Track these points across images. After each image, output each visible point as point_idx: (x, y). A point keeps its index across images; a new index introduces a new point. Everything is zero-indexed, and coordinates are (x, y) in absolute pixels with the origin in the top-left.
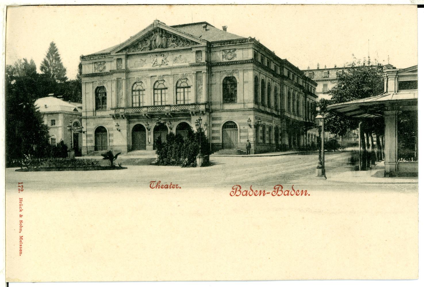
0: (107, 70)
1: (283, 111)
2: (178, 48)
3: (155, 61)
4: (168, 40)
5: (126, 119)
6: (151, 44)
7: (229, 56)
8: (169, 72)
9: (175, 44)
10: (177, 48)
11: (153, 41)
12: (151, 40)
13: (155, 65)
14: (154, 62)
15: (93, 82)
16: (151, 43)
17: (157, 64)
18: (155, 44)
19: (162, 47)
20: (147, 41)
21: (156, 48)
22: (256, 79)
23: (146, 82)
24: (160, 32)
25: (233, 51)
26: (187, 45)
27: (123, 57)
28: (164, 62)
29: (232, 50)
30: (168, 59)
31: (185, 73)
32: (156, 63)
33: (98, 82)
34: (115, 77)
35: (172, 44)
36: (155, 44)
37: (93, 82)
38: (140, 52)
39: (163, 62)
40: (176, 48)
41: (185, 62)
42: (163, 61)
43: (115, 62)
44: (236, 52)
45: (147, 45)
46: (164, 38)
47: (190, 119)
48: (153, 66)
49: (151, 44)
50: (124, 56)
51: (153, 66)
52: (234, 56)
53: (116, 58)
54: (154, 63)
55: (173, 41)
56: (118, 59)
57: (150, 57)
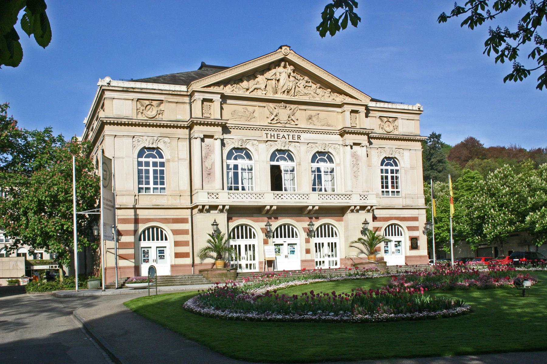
2: (317, 100)
4: (298, 84)
9: (313, 94)
12: (270, 78)
13: (274, 122)
15: (134, 137)
17: (278, 121)
24: (285, 67)
26: (331, 98)
27: (217, 98)
28: (292, 120)
30: (299, 114)
31: (327, 143)
32: (276, 118)
33: (147, 137)
38: (247, 94)
39: (290, 119)
40: (313, 99)
46: (292, 79)
48: (271, 123)
50: (219, 96)
51: (271, 123)
54: (274, 119)
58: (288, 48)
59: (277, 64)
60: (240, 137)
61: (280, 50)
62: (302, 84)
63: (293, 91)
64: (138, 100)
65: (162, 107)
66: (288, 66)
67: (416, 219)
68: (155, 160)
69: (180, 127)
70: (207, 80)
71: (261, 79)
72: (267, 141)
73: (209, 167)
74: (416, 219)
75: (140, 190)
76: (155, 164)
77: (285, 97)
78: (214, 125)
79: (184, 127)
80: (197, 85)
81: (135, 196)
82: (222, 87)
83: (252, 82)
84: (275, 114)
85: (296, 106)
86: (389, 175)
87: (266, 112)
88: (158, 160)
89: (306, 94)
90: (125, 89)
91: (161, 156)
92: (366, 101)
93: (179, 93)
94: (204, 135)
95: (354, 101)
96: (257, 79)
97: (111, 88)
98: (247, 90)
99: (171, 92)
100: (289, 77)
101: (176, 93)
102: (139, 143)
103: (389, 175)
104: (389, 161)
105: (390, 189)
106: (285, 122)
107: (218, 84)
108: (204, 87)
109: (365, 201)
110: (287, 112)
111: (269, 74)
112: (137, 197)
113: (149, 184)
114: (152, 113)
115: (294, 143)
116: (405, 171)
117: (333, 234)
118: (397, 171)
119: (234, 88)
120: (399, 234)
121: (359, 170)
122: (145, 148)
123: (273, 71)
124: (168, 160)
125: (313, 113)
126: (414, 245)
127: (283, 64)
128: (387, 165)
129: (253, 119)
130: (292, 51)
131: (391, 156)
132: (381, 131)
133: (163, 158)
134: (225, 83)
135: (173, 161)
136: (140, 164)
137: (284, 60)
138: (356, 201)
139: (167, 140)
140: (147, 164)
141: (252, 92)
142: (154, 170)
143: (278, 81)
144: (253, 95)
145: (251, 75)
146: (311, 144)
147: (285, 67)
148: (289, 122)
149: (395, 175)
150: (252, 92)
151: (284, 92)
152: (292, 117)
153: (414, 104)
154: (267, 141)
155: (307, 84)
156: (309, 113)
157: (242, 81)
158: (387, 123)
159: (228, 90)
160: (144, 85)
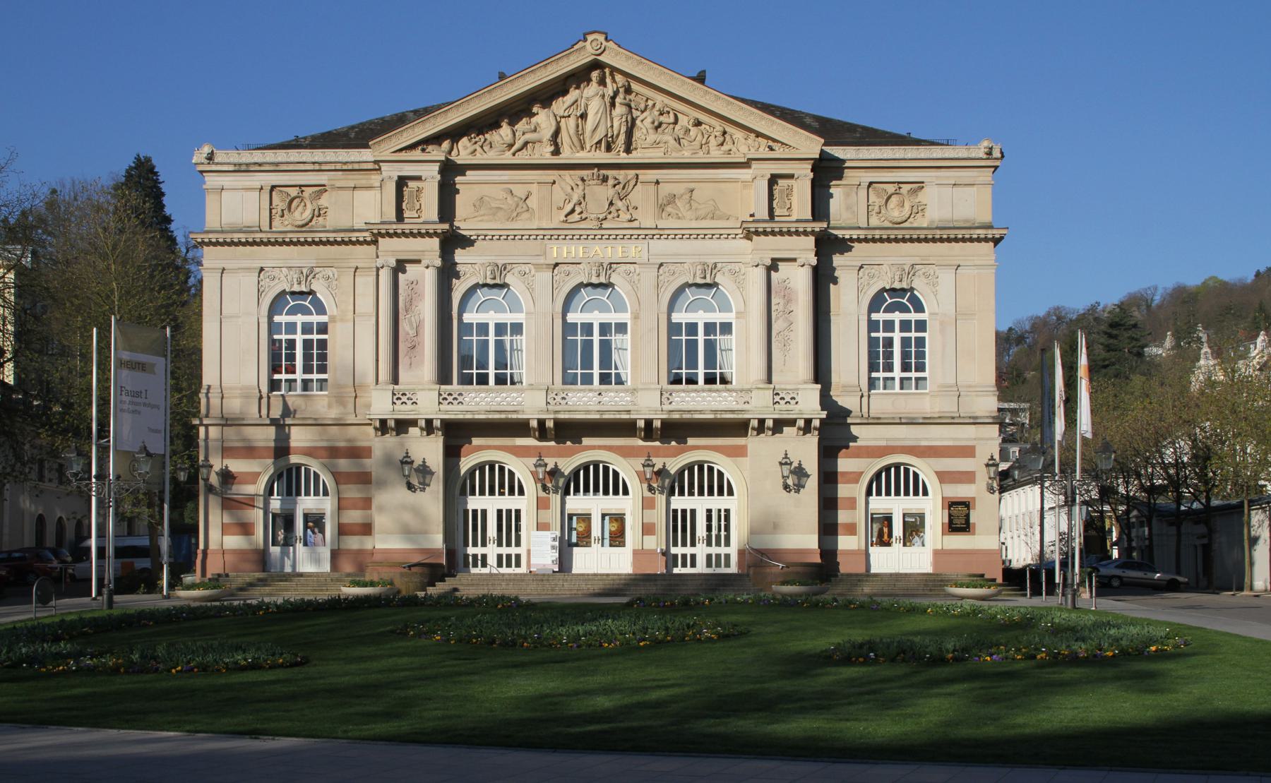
2: (686, 155)
3: (575, 200)
5: (441, 439)
6: (557, 133)
7: (895, 212)
8: (634, 250)
9: (672, 142)
10: (679, 155)
11: (572, 122)
13: (576, 217)
14: (568, 208)
16: (558, 123)
17: (584, 216)
18: (579, 133)
20: (534, 115)
21: (582, 148)
23: (530, 289)
24: (602, 82)
25: (913, 192)
26: (725, 147)
27: (432, 173)
29: (909, 187)
31: (711, 261)
32: (578, 209)
33: (284, 268)
34: (392, 249)
35: (652, 137)
36: (579, 133)
37: (262, 269)
38: (508, 158)
39: (612, 209)
40: (674, 154)
41: (712, 218)
42: (611, 204)
43: (391, 188)
44: (923, 197)
45: (535, 131)
46: (619, 110)
49: (557, 133)
50: (436, 167)
52: (915, 210)
53: (391, 172)
54: (573, 211)
57: (554, 182)
58: (601, 38)
59: (579, 77)
60: (493, 259)
61: (581, 44)
62: (649, 120)
63: (622, 138)
64: (273, 188)
65: (324, 201)
66: (608, 80)
67: (968, 451)
68: (307, 319)
69: (360, 243)
70: (405, 134)
71: (543, 119)
72: (557, 265)
73: (412, 333)
74: (968, 451)
75: (274, 385)
76: (307, 329)
77: (601, 157)
78: (428, 235)
79: (365, 242)
80: (384, 148)
81: (261, 398)
82: (446, 145)
83: (522, 125)
84: (575, 199)
85: (632, 173)
86: (897, 336)
87: (558, 194)
88: (315, 319)
89: (657, 143)
90: (243, 168)
91: (321, 310)
92: (811, 146)
93: (356, 166)
94: (398, 261)
95: (779, 152)
96: (534, 120)
97: (214, 168)
98: (511, 146)
99: (339, 166)
100: (613, 105)
101: (350, 167)
102: (272, 284)
103: (897, 336)
104: (897, 297)
105: (897, 373)
106: (601, 217)
107: (436, 139)
108: (401, 150)
109: (788, 407)
110: (607, 192)
111: (560, 105)
112: (264, 401)
113: (294, 372)
114: (301, 214)
115: (623, 267)
116: (942, 323)
117: (724, 488)
118: (921, 326)
119: (477, 147)
120: (919, 488)
121: (792, 327)
122: (283, 293)
123: (573, 94)
124: (333, 319)
125: (679, 189)
126: (959, 519)
127: (595, 75)
128: (890, 309)
129: (525, 215)
130: (611, 44)
131: (897, 285)
132: (874, 221)
133: (324, 313)
134: (454, 134)
135: (342, 320)
136: (273, 328)
137: (596, 65)
138: (759, 405)
139: (329, 272)
140: (291, 328)
141: (520, 150)
142: (305, 341)
143: (584, 116)
144: (522, 158)
145: (517, 110)
146: (672, 267)
147: (602, 82)
148: (610, 217)
149: (913, 335)
150: (520, 150)
151: (599, 142)
152: (619, 204)
153: (977, 142)
154: (557, 265)
155: (662, 119)
156: (665, 189)
157: (497, 126)
158: (894, 199)
159: (464, 151)
160: (281, 155)
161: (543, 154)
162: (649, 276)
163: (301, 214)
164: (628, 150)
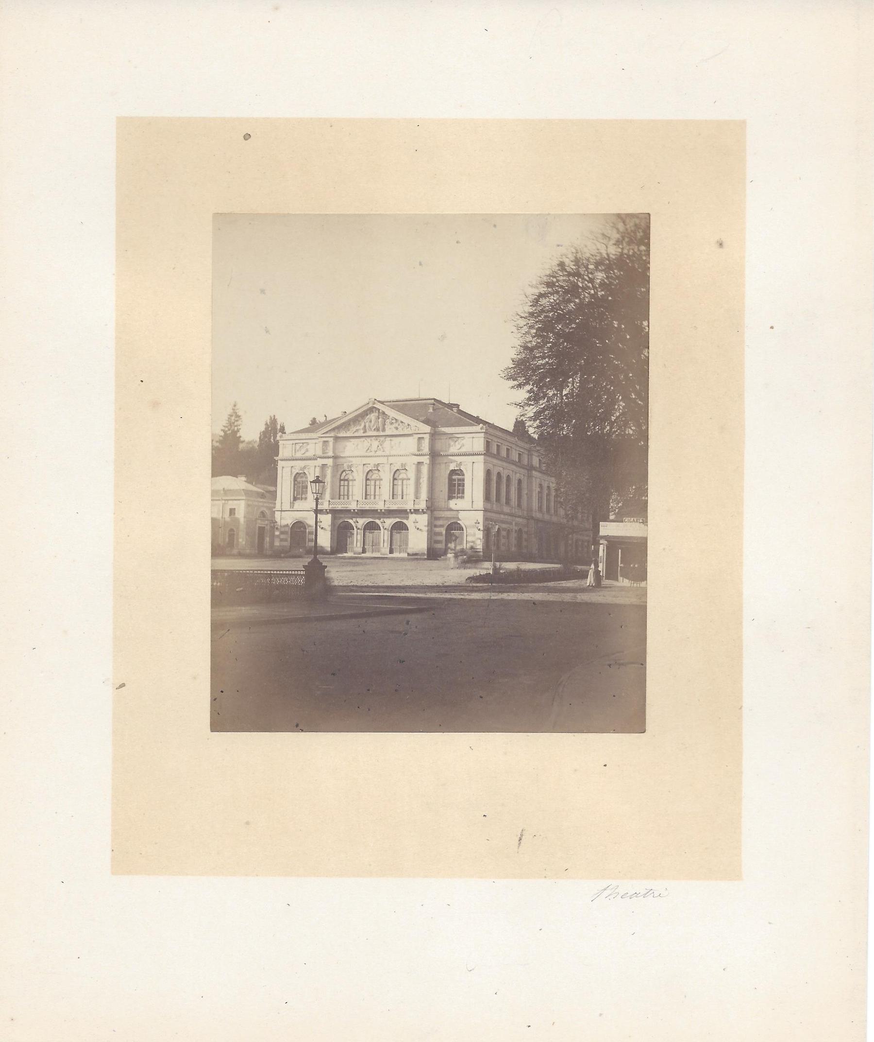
0: (310, 454)
1: (530, 510)
8: (384, 460)
19: (378, 430)
22: (488, 473)
34: (321, 462)
47: (407, 518)
55: (392, 423)
56: (325, 442)
77: (376, 433)
107: (333, 429)
114: (303, 451)
138: (409, 506)
144: (356, 434)
145: (356, 420)
161: (361, 433)
162: (387, 467)
163: (303, 451)
164: (384, 430)
